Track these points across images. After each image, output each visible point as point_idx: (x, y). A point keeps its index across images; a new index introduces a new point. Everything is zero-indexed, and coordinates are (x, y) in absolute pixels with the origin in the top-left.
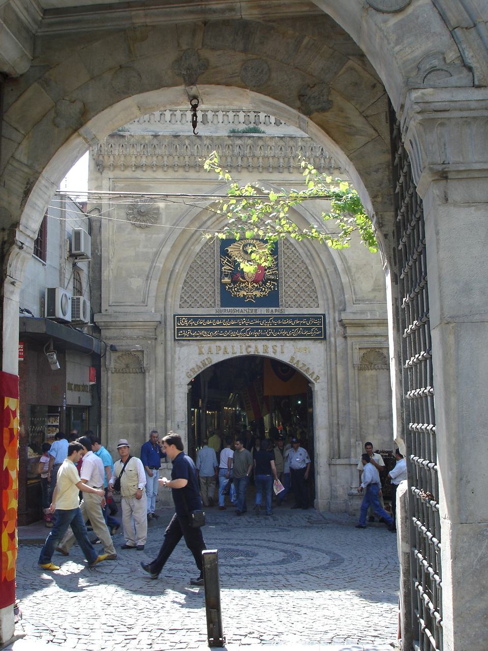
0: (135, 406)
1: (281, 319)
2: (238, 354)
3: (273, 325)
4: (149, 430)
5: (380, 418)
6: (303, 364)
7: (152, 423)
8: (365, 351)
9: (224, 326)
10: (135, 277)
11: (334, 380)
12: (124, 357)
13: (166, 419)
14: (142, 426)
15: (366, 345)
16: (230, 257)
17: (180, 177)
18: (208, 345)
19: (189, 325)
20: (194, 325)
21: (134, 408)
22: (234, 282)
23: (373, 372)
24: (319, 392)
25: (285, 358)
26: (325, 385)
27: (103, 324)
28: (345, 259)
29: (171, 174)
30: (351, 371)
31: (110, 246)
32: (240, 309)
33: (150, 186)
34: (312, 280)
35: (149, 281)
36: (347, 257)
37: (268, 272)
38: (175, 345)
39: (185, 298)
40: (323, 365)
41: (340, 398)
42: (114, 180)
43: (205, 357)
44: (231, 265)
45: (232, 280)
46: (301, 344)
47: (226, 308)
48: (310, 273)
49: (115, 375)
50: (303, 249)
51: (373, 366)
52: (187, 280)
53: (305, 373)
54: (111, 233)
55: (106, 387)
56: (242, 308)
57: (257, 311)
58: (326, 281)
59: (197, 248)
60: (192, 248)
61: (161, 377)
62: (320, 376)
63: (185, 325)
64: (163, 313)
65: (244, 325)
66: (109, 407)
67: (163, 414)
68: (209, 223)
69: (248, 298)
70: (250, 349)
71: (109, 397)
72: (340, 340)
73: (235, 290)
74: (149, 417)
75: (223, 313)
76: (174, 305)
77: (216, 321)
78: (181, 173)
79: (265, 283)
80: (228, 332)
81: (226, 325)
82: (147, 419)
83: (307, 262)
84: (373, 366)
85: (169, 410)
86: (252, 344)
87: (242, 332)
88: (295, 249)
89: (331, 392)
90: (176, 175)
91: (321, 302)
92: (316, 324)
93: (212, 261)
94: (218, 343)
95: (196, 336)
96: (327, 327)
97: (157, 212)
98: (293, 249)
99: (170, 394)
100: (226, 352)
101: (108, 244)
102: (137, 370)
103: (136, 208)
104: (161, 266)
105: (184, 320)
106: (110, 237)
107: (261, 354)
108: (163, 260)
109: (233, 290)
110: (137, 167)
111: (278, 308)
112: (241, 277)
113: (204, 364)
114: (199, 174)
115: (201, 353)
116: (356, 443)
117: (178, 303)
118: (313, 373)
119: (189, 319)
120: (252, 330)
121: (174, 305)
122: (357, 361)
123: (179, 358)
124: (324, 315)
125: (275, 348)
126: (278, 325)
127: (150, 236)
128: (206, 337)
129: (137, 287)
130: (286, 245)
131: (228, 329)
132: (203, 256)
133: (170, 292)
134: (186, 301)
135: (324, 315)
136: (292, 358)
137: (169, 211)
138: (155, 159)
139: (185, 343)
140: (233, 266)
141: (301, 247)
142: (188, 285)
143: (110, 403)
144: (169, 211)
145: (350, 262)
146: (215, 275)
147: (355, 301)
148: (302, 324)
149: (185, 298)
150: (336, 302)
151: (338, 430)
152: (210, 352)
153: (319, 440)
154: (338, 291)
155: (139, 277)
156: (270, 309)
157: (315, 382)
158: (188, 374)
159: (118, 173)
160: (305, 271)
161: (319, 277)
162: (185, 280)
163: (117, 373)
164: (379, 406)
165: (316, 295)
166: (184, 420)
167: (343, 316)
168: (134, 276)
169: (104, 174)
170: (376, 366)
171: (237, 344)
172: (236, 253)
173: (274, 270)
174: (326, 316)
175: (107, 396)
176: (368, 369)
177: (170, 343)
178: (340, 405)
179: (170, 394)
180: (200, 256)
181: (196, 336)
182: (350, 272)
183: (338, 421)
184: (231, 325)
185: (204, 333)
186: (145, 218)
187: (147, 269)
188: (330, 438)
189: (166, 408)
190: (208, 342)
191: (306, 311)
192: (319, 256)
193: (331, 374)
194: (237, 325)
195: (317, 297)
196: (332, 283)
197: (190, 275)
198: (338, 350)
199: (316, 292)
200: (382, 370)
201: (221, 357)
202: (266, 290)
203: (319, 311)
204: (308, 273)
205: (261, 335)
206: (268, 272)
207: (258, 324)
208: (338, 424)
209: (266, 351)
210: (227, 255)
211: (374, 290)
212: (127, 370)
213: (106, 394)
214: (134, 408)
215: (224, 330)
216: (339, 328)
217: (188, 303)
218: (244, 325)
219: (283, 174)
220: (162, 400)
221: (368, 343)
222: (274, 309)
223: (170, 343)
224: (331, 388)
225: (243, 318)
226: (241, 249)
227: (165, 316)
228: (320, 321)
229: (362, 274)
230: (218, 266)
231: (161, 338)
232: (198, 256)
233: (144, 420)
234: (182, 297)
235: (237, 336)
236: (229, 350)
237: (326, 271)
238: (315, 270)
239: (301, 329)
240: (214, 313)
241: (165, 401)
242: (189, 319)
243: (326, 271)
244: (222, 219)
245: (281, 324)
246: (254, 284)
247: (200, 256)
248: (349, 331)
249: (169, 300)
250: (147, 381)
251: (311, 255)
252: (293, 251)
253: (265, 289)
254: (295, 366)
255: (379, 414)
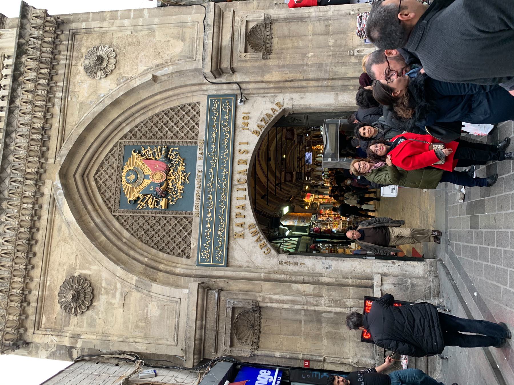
0: (301, 321)
1: (209, 144)
2: (246, 193)
3: (216, 153)
4: (331, 306)
5: (327, 33)
6: (261, 120)
7: (323, 303)
8: (249, 48)
9: (213, 206)
10: (147, 310)
11: (282, 85)
12: (239, 332)
13: (318, 283)
14: (323, 315)
15: (243, 45)
16: (138, 198)
17: (42, 249)
18: (234, 226)
19: (210, 248)
20: (210, 243)
21: (303, 323)
22: (165, 194)
23: (275, 41)
24: (295, 103)
25: (254, 140)
26: (288, 96)
27: (196, 357)
28: (148, 69)
29: (37, 261)
30: (271, 62)
31: (109, 338)
32: (196, 189)
33: (49, 285)
34: (171, 109)
35: (152, 294)
36: (146, 68)
37: (158, 156)
38: (233, 266)
39: (180, 251)
40: (264, 99)
41: (302, 78)
42: (36, 328)
43: (247, 232)
44: (147, 198)
45: (164, 197)
46: (240, 121)
47: (194, 205)
48: (163, 112)
49: (260, 344)
50: (137, 118)
51: (268, 41)
52: (160, 247)
53: (272, 119)
54: (94, 337)
55: (275, 358)
56: (196, 186)
57: (200, 170)
58: (170, 93)
59: (126, 234)
60: (124, 240)
61: (267, 285)
62: (276, 102)
63: (210, 253)
64: (192, 278)
65: (214, 185)
66: (301, 356)
67: (312, 287)
68: (98, 220)
69: (185, 180)
70: (242, 180)
71: (288, 357)
72: (238, 78)
73: (176, 194)
74: (314, 305)
75: (199, 209)
76: (186, 265)
77: (207, 217)
78: (38, 249)
79: (170, 161)
80: (220, 204)
81: (212, 206)
82: (317, 308)
83: (150, 114)
84: (268, 41)
85: (306, 279)
86: (236, 176)
87: (221, 187)
88: (137, 127)
89: (295, 88)
90: (39, 255)
91: (195, 100)
92: (218, 105)
93: (141, 218)
94: (233, 214)
95: (223, 240)
96: (222, 92)
97: (76, 279)
98: (136, 129)
99: (288, 277)
100: (244, 207)
101: (106, 341)
102: (256, 315)
103: (70, 304)
104: (135, 278)
105: (204, 254)
106: (98, 338)
107: (247, 167)
108: (131, 275)
109: (175, 196)
110: (24, 300)
111: (199, 147)
112: (161, 186)
113: (255, 234)
114: (41, 228)
115: (243, 236)
116: (357, 56)
117: (184, 260)
118: (272, 109)
119: (203, 248)
120: (220, 176)
121: (186, 265)
122: (261, 54)
123: (247, 262)
124: (209, 96)
125: (242, 151)
126: (216, 148)
127: (103, 289)
128: (224, 229)
129: (158, 308)
130: (131, 137)
131: (218, 204)
132: (135, 229)
133: (169, 269)
134: (182, 251)
135: (209, 96)
136: (255, 132)
137: (78, 265)
138: (16, 279)
139: (230, 255)
140: (149, 196)
141: (134, 120)
142: (165, 248)
143: (294, 356)
144: (78, 265)
145: (150, 65)
146: (157, 217)
147: (192, 58)
148: (217, 120)
149: (180, 251)
150: (195, 81)
151: (340, 79)
152: (242, 225)
153: (350, 103)
154: (182, 79)
155: (147, 306)
156: (198, 155)
157: (283, 108)
158: (266, 252)
159: (29, 323)
160: (160, 116)
161: (166, 101)
162: (160, 250)
163: (259, 341)
164: (313, 35)
165: (187, 106)
166: (320, 261)
167: (207, 70)
168: (146, 311)
169: (29, 341)
170: (268, 37)
171: (235, 194)
172: (136, 191)
173: (157, 151)
174: (210, 93)
175: (286, 358)
176: (271, 46)
177: (229, 272)
178: (311, 76)
179: (288, 277)
180: (135, 232)
181: (223, 240)
182: (162, 64)
183: (329, 79)
184: (213, 200)
185: (221, 231)
186: (82, 294)
187: (138, 295)
188: (350, 90)
189: (304, 282)
190: (231, 227)
191: (203, 117)
192: (145, 100)
193: (275, 88)
194: (213, 193)
195: (190, 105)
196: (174, 86)
197: (155, 244)
198: (247, 80)
199: (184, 106)
200: (273, 31)
201: (249, 213)
202: (177, 160)
203: (204, 102)
204: (163, 114)
205: (227, 167)
206: (158, 156)
207: (214, 169)
208: (333, 79)
209: (245, 162)
210: (136, 201)
211: (183, 40)
212: (256, 328)
213: (284, 360)
214: (303, 323)
215: (218, 208)
216: (223, 79)
217: (185, 248)
218: (214, 185)
219: (52, 136)
220: (295, 286)
221: (240, 45)
222: (199, 152)
223: (229, 272)
224: (291, 88)
225: (206, 186)
226: (130, 186)
227: (197, 276)
228: (215, 101)
229: (164, 51)
230: (148, 213)
231: (221, 284)
232: (134, 234)
233: (320, 313)
234: (179, 255)
235: (226, 194)
236: (241, 203)
237: (161, 93)
238: (160, 105)
239: (222, 122)
240: (198, 219)
241: (296, 282)
242: (203, 248)
243: (161, 93)
244: (96, 205)
245: (216, 144)
246: (170, 172)
247: (135, 232)
248: (225, 64)
249: (178, 270)
250: (269, 305)
251: (142, 108)
252: (139, 130)
253: (176, 161)
254: (263, 130)
255: (322, 34)
